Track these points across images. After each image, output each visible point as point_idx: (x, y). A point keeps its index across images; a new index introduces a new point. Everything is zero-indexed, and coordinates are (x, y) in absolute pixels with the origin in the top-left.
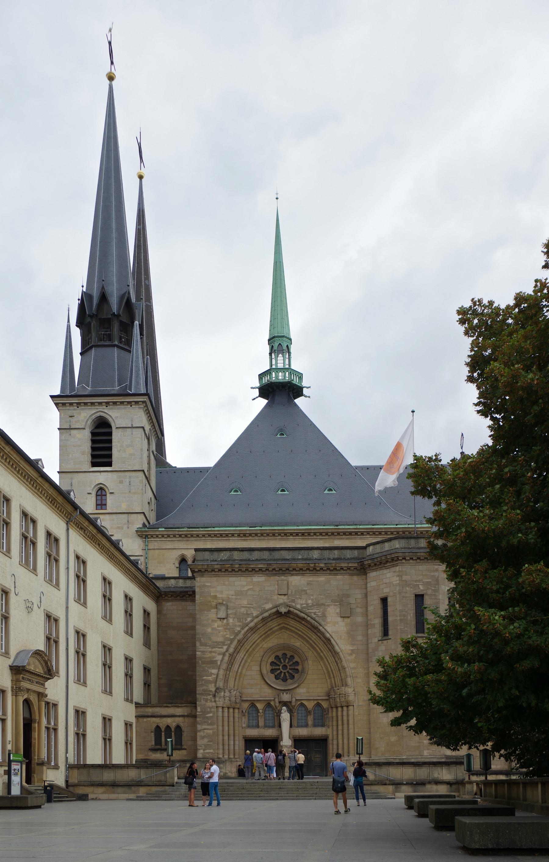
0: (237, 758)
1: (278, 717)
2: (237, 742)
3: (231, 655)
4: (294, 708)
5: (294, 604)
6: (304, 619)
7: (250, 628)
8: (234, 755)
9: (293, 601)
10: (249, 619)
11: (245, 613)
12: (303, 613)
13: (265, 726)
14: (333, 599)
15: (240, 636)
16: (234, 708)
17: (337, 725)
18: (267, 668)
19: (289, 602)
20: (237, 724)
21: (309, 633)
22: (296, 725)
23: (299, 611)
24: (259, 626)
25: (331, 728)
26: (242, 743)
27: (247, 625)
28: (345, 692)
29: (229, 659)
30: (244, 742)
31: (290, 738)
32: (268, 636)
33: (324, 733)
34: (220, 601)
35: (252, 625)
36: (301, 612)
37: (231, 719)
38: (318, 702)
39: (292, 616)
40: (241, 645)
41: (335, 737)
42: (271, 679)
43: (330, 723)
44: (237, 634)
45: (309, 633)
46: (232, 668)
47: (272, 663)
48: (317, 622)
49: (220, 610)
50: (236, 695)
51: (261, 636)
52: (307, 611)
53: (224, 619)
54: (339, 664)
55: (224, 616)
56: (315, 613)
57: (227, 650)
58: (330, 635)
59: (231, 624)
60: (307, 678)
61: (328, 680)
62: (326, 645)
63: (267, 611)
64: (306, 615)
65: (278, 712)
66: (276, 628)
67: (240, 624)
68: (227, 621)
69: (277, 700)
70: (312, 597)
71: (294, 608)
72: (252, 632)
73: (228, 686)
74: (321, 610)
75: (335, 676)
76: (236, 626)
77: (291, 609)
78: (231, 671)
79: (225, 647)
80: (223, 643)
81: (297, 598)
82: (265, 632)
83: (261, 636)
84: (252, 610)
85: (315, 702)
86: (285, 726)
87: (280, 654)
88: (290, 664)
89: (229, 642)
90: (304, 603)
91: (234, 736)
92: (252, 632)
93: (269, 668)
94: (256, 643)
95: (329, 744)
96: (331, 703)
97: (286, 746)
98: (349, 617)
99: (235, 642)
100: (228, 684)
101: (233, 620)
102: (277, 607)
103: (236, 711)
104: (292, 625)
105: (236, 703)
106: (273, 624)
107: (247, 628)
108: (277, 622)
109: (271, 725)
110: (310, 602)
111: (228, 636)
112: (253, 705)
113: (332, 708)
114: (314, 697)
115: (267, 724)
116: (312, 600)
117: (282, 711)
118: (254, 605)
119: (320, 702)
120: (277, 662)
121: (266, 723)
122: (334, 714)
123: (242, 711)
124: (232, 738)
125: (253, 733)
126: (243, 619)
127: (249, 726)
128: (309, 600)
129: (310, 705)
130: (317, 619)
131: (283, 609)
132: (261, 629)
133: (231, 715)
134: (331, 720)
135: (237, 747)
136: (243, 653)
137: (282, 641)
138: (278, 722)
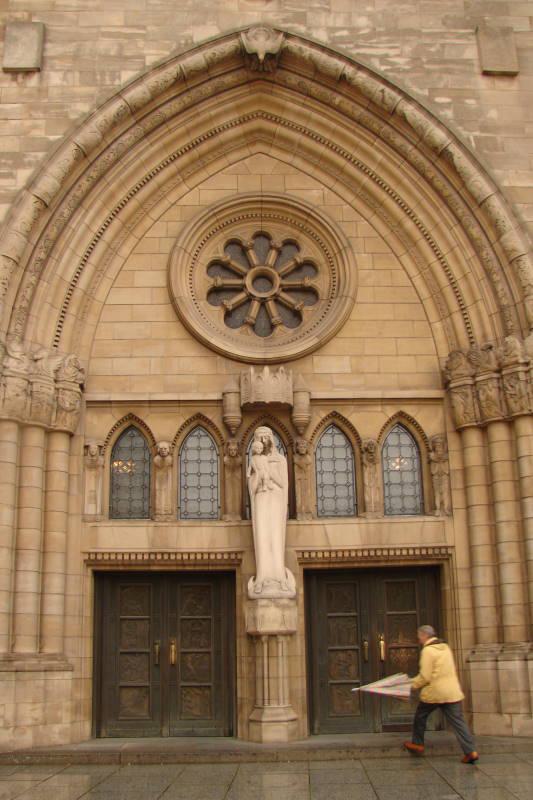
0: (52, 657)
1: (238, 474)
2: (55, 583)
3: (44, 206)
4: (300, 435)
5: (301, 29)
6: (343, 79)
7: (135, 111)
8: (40, 639)
9: (301, 18)
10: (127, 76)
11: (113, 53)
12: (341, 57)
13: (182, 514)
14: (447, 17)
15: (89, 134)
16: (49, 432)
17: (492, 505)
18: (193, 283)
19: (285, 21)
20: (58, 501)
21: (356, 146)
22: (313, 509)
23: (323, 49)
24: (167, 110)
25: (459, 515)
26: (83, 587)
27: (119, 95)
28: (525, 354)
29: (36, 220)
30: (88, 584)
31: (287, 564)
32: (200, 163)
33: (430, 542)
34: (19, 15)
35: (138, 93)
36: (332, 53)
37: (34, 477)
38: (401, 414)
39: (293, 79)
40: (93, 173)
41: (483, 555)
42: (209, 321)
43: (458, 499)
44: (77, 127)
45: (356, 146)
46: (52, 263)
47: (216, 265)
48: (394, 87)
49: (16, 39)
50: (62, 376)
51: (173, 159)
52: (355, 52)
53: (28, 72)
54: (487, 253)
55: (29, 62)
56: (383, 59)
57: (31, 184)
58: (450, 133)
59: (54, 92)
60: (353, 316)
61: (438, 326)
62: (430, 182)
63: (200, 47)
64: (351, 62)
65: (239, 453)
66: (231, 133)
67: (92, 90)
68: (41, 79)
69: (232, 402)
70: (369, 9)
71: (304, 41)
72: (139, 130)
73: (29, 337)
74: (408, 49)
75: (468, 301)
76: (73, 98)
77: (293, 44)
78: (47, 274)
79: (24, 175)
80: (17, 160)
81: (312, 9)
82: (187, 141)
83: (173, 159)
84: (141, 43)
85: (391, 411)
86: (269, 511)
87: (245, 233)
88: (282, 269)
89: (41, 155)
90: (340, 23)
91: (44, 552)
92: (139, 130)
93: (204, 282)
94: (152, 185)
95: (454, 587)
96: (460, 409)
97: (274, 600)
98: (510, 75)
99: (68, 155)
100: (30, 329)
101: (65, 79)
102: (237, 34)
103: (60, 443)
104: (291, 118)
105: (60, 409)
106: (223, 113)
107: (116, 107)
108: (238, 108)
109: (206, 508)
110: (362, 22)
111: (38, 133)
112: (132, 425)
113: (460, 431)
114: (380, 388)
115: (192, 507)
116: (370, 16)
117: (258, 445)
118: (149, 28)
119: (409, 410)
120: (237, 265)
121: (186, 501)
122: (475, 457)
123: (87, 447)
124: (30, 562)
125: (129, 540)
126: (103, 73)
127: (114, 514)
128: (360, 15)
129: (368, 424)
130: (390, 76)
131: (262, 39)
132: (172, 124)
133: (35, 458)
134: (459, 485)
135: (54, 606)
136: (99, 213)
137: (252, 186)
138: (238, 492)
